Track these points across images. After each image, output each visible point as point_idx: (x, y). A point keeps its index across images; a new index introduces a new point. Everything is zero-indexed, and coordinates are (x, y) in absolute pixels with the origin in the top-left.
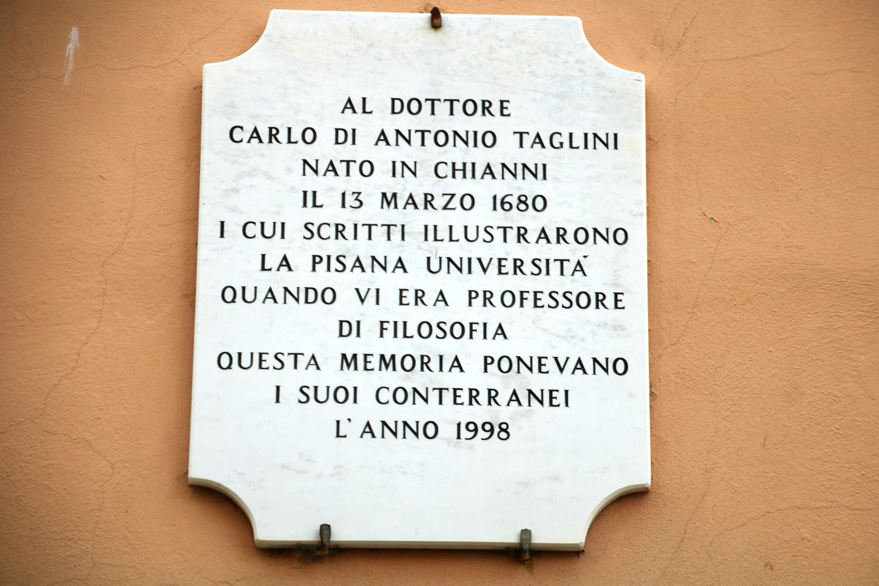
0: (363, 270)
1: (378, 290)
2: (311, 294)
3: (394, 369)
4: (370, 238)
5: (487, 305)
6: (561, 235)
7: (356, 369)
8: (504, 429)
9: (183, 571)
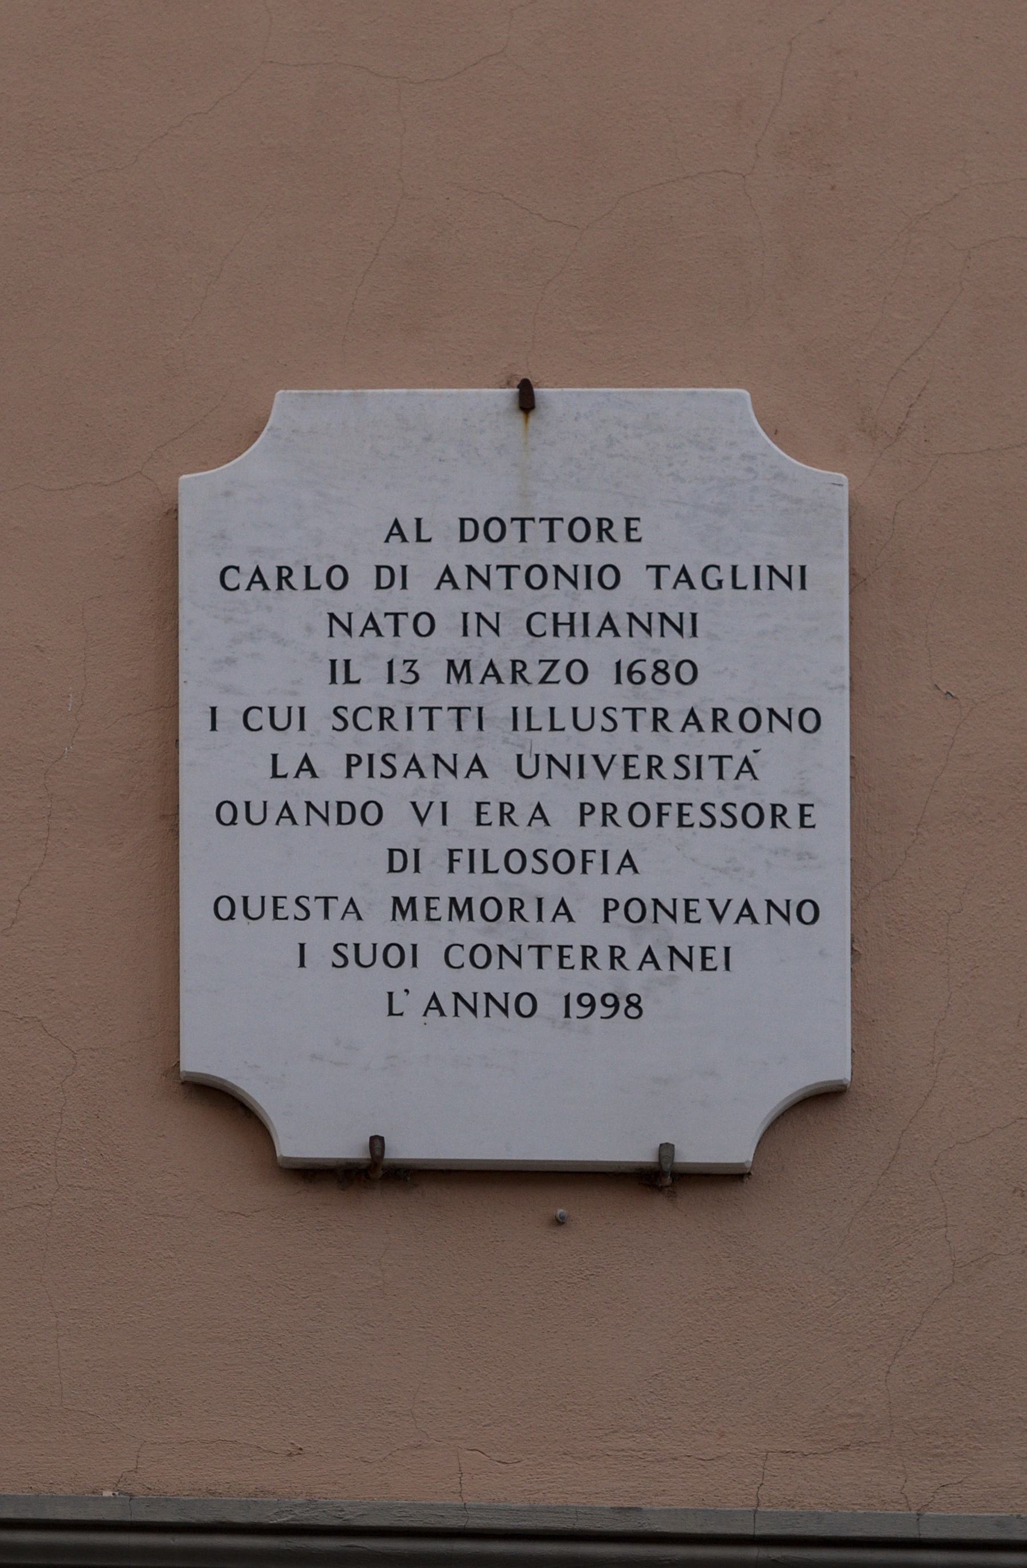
0: (422, 775)
1: (444, 804)
2: (346, 810)
3: (471, 918)
4: (431, 728)
5: (608, 824)
6: (719, 719)
7: (414, 918)
8: (634, 1003)
9: (180, 1198)
